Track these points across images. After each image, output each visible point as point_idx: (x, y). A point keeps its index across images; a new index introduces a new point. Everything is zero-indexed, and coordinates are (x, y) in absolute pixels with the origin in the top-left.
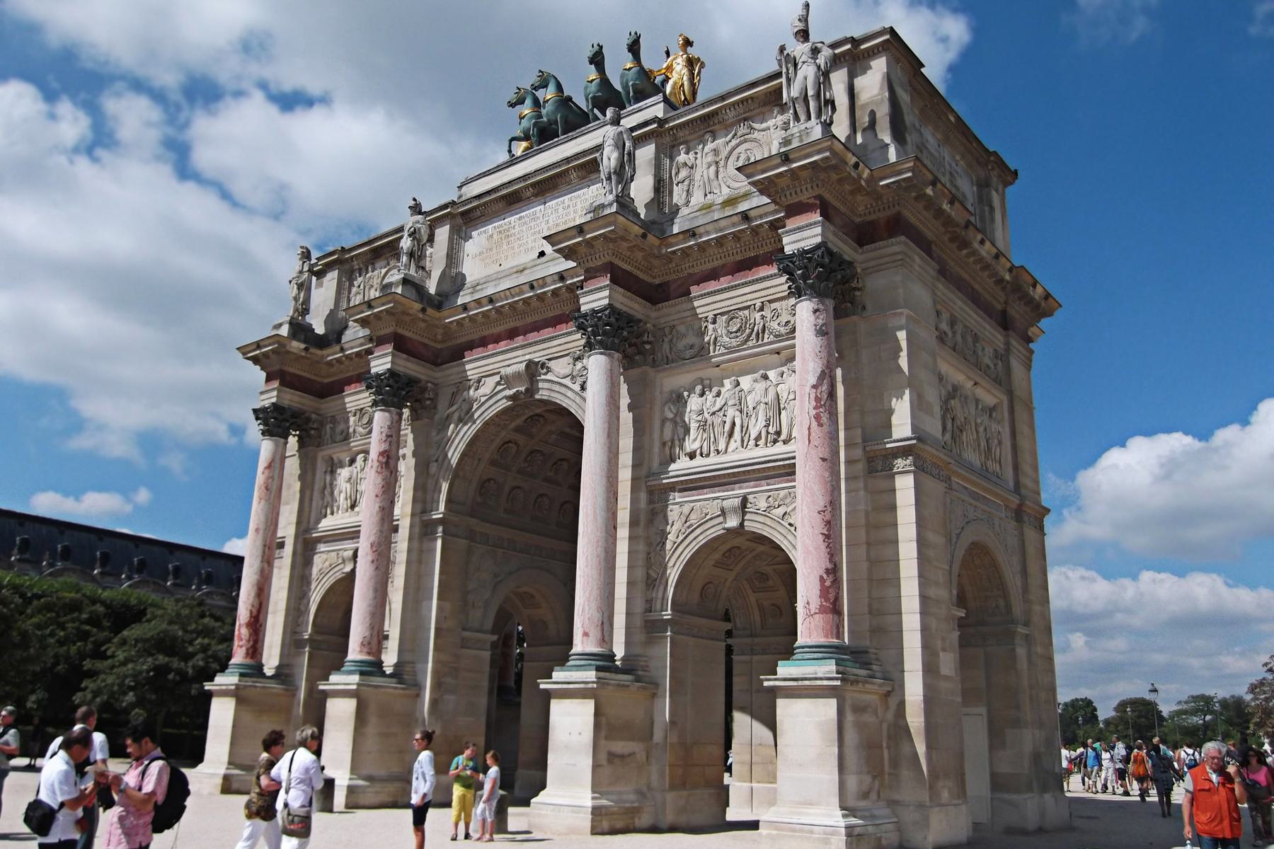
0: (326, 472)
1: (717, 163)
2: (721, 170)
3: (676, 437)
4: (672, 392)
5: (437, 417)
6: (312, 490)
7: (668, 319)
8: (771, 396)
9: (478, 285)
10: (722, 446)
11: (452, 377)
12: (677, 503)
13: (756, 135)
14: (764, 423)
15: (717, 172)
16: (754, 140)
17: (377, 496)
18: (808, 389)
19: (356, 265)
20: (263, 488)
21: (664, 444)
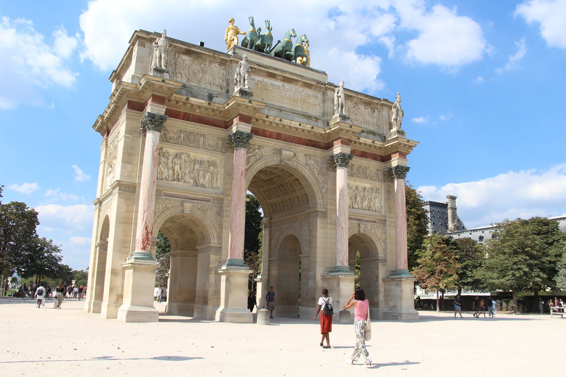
1: (349, 113)
8: (370, 197)
10: (354, 206)
14: (367, 203)
20: (156, 159)
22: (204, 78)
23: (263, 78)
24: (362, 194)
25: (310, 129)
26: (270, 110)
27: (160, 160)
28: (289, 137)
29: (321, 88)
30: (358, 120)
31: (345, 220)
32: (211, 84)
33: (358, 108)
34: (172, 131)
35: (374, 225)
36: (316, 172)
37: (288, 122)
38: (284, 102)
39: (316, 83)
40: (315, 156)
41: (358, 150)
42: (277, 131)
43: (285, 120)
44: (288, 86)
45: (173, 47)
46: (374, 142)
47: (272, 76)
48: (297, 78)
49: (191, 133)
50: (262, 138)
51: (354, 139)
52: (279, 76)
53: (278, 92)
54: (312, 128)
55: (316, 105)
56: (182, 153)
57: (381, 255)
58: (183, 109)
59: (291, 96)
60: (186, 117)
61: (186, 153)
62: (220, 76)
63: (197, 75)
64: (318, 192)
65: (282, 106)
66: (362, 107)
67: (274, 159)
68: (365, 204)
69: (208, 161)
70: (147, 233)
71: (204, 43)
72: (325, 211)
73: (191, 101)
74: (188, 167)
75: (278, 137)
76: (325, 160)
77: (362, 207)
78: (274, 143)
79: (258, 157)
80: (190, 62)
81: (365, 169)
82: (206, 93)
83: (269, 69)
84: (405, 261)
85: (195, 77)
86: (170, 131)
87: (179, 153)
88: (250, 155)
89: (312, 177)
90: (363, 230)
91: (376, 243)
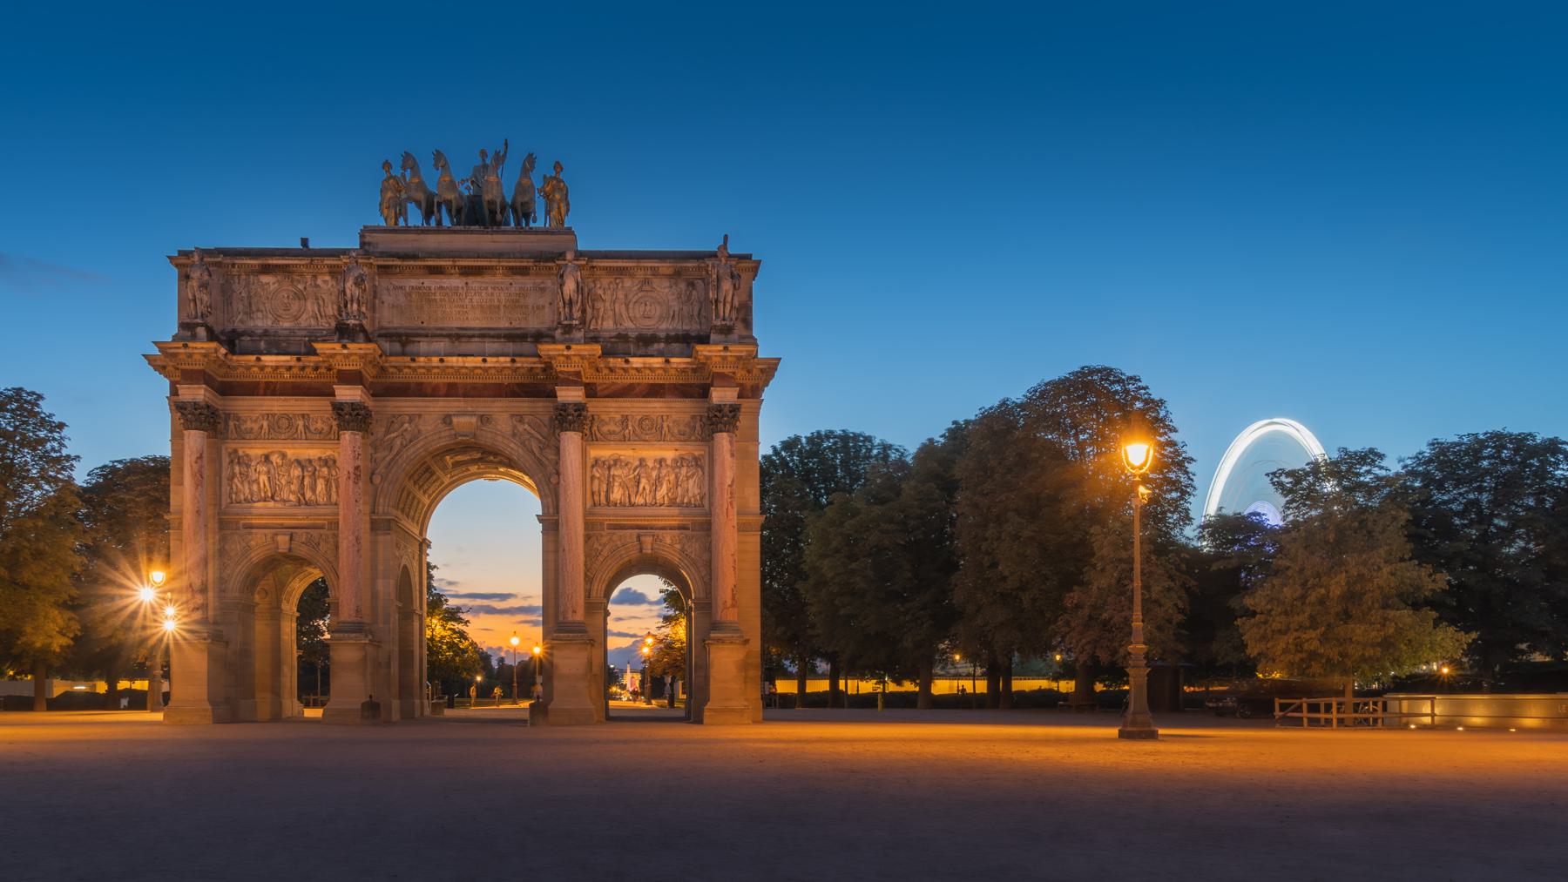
0: (232, 462)
2: (630, 311)
4: (596, 461)
6: (220, 478)
7: (595, 409)
8: (672, 477)
11: (389, 409)
14: (665, 491)
18: (726, 487)
19: (235, 271)
21: (593, 493)
23: (421, 281)
24: (654, 474)
25: (509, 365)
33: (649, 289)
41: (639, 384)
42: (446, 381)
43: (450, 358)
44: (474, 282)
47: (436, 271)
48: (489, 264)
54: (513, 361)
55: (543, 307)
56: (272, 452)
60: (271, 390)
67: (443, 434)
68: (663, 491)
69: (320, 459)
74: (284, 476)
75: (451, 391)
78: (441, 404)
79: (408, 437)
80: (276, 285)
81: (660, 421)
85: (287, 312)
90: (649, 547)
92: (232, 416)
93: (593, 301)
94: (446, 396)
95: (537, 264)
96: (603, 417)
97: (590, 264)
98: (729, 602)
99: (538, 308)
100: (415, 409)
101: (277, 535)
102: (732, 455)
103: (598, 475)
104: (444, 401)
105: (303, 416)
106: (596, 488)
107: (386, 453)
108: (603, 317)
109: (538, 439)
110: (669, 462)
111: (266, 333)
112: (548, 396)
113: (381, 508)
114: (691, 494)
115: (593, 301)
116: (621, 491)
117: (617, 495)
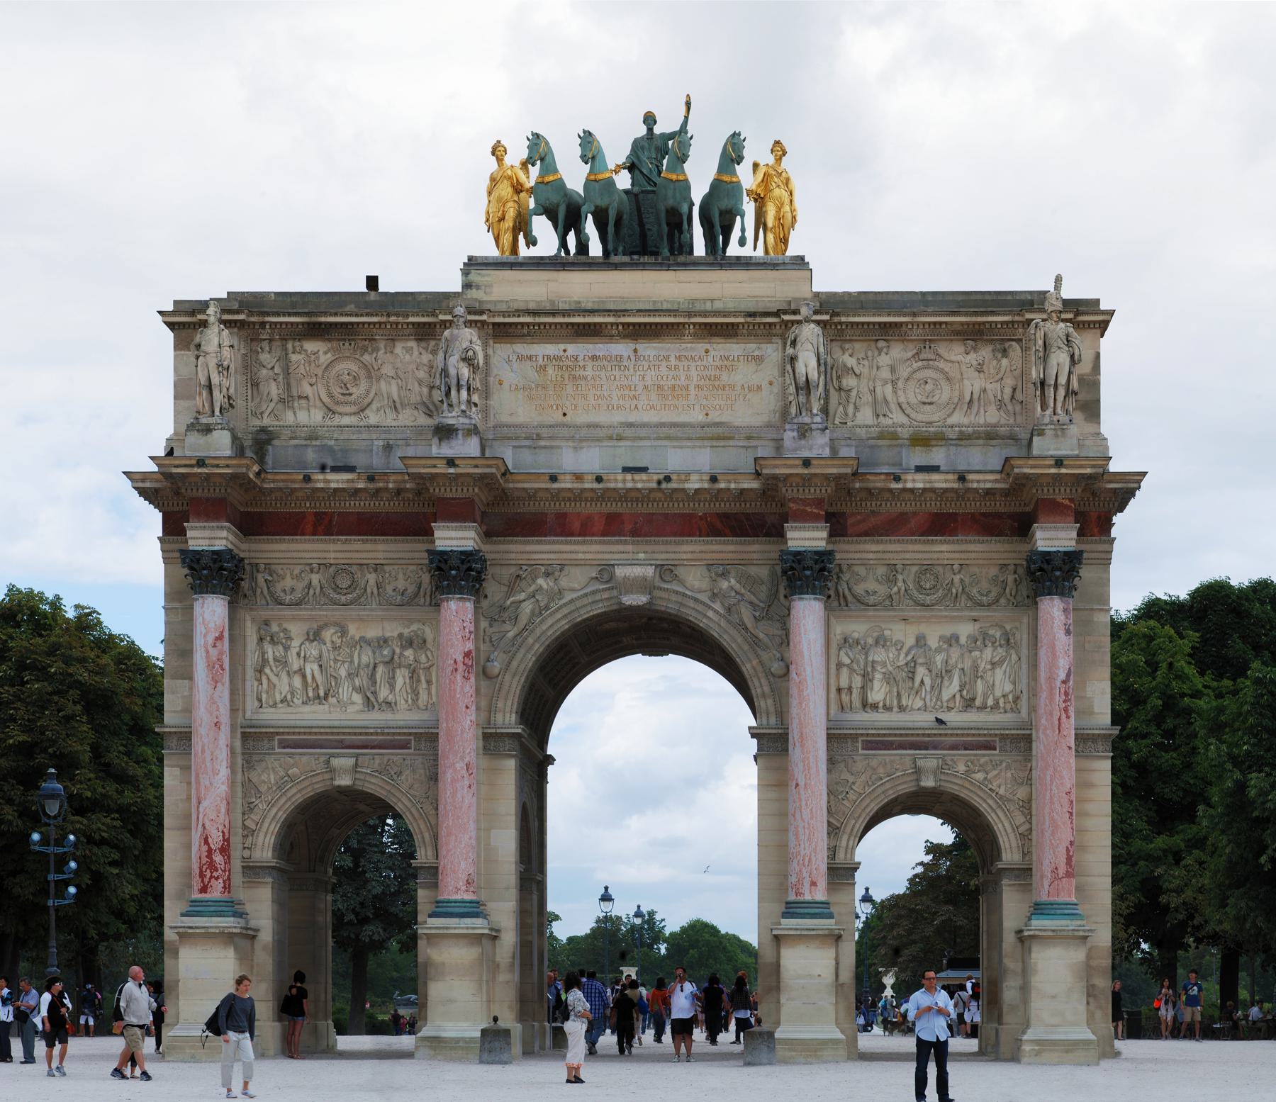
0: (261, 639)
2: (900, 393)
3: (853, 685)
5: (485, 604)
8: (967, 664)
9: (539, 437)
10: (904, 702)
11: (513, 556)
12: (861, 755)
13: (942, 364)
14: (958, 688)
15: (895, 392)
16: (941, 371)
17: (467, 707)
18: (1058, 684)
21: (839, 690)
22: (372, 395)
23: (562, 346)
24: (939, 659)
25: (706, 486)
26: (581, 448)
27: (263, 656)
28: (650, 518)
29: (770, 324)
30: (935, 399)
31: (803, 762)
32: (395, 407)
33: (931, 356)
34: (288, 572)
35: (984, 755)
36: (746, 615)
37: (624, 481)
38: (639, 407)
39: (745, 316)
40: (742, 562)
41: (915, 514)
44: (649, 349)
45: (268, 327)
46: (962, 478)
49: (343, 569)
50: (554, 542)
51: (879, 485)
52: (609, 327)
53: (618, 378)
54: (714, 479)
55: (760, 388)
57: (1010, 855)
58: (308, 505)
59: (665, 378)
61: (336, 624)
62: (422, 374)
63: (351, 391)
64: (757, 675)
65: (632, 419)
66: (954, 354)
67: (598, 597)
69: (401, 636)
70: (210, 851)
71: (377, 277)
72: (780, 731)
73: (318, 481)
75: (612, 526)
76: (779, 569)
77: (939, 703)
80: (329, 355)
82: (376, 443)
83: (569, 316)
84: (1053, 872)
86: (281, 572)
87: (315, 626)
88: (522, 596)
89: (734, 633)
91: (992, 818)
92: (262, 566)
93: (838, 377)
94: (605, 533)
95: (749, 320)
96: (856, 569)
97: (836, 319)
98: (1062, 872)
99: (751, 389)
100: (552, 556)
101: (333, 755)
102: (1068, 632)
103: (847, 661)
104: (601, 542)
105: (377, 568)
106: (844, 683)
107: (507, 627)
108: (855, 404)
109: (751, 603)
110: (963, 640)
111: (313, 437)
112: (767, 535)
113: (499, 718)
114: (998, 693)
115: (838, 377)
116: (885, 688)
117: (877, 694)
